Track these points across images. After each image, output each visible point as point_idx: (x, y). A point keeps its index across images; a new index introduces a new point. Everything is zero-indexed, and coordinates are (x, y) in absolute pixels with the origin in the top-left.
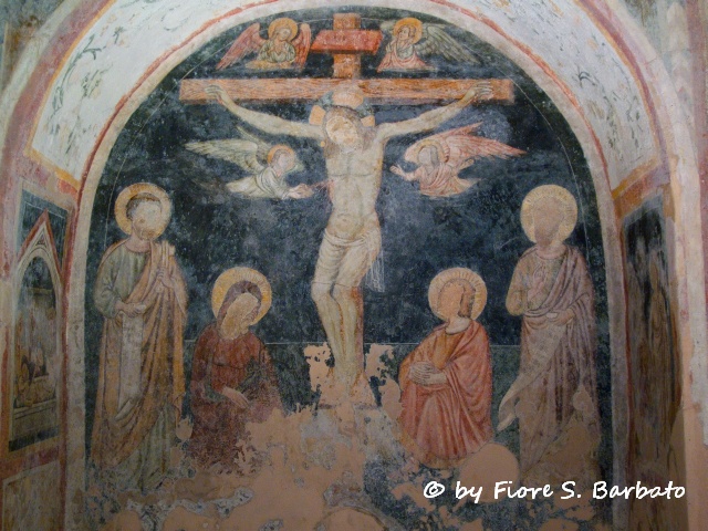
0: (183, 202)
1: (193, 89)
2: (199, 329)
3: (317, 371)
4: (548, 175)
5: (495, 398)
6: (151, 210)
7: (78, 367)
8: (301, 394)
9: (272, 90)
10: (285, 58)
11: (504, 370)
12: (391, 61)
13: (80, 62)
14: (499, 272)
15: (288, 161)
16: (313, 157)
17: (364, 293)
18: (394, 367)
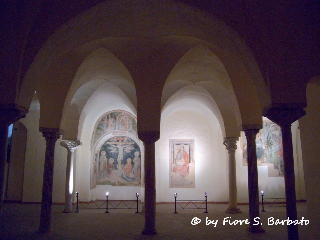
0: (107, 153)
1: (108, 143)
2: (108, 163)
3: (118, 167)
4: (137, 151)
5: (132, 169)
6: (104, 153)
7: (98, 165)
8: (116, 169)
9: (114, 143)
10: (116, 141)
11: (133, 167)
12: (124, 141)
13: (100, 143)
14: (133, 159)
15: (116, 150)
16: (118, 149)
17: (122, 161)
18: (124, 167)
